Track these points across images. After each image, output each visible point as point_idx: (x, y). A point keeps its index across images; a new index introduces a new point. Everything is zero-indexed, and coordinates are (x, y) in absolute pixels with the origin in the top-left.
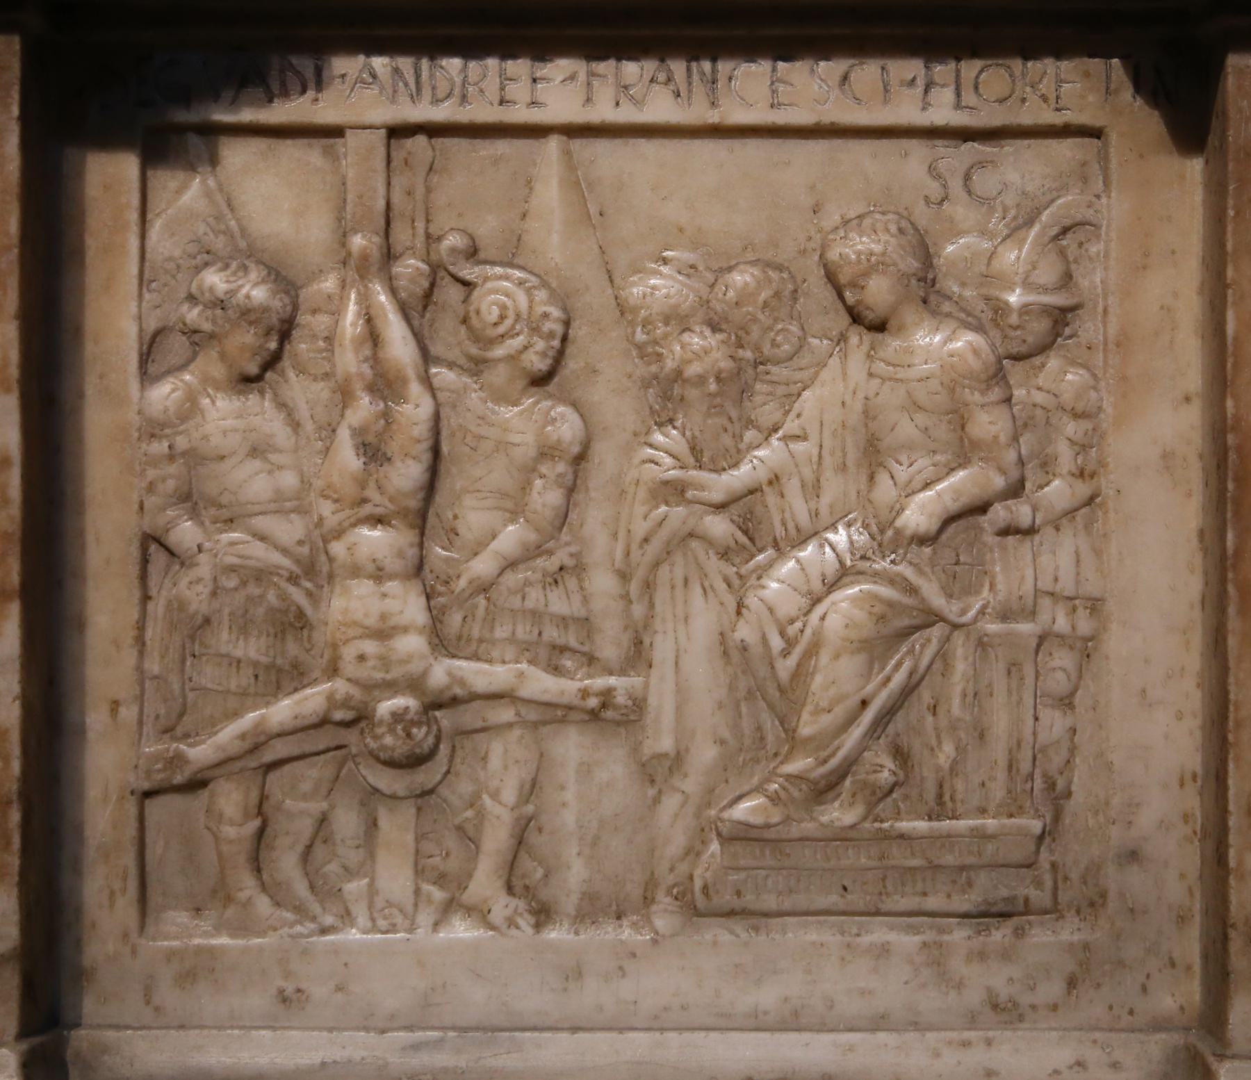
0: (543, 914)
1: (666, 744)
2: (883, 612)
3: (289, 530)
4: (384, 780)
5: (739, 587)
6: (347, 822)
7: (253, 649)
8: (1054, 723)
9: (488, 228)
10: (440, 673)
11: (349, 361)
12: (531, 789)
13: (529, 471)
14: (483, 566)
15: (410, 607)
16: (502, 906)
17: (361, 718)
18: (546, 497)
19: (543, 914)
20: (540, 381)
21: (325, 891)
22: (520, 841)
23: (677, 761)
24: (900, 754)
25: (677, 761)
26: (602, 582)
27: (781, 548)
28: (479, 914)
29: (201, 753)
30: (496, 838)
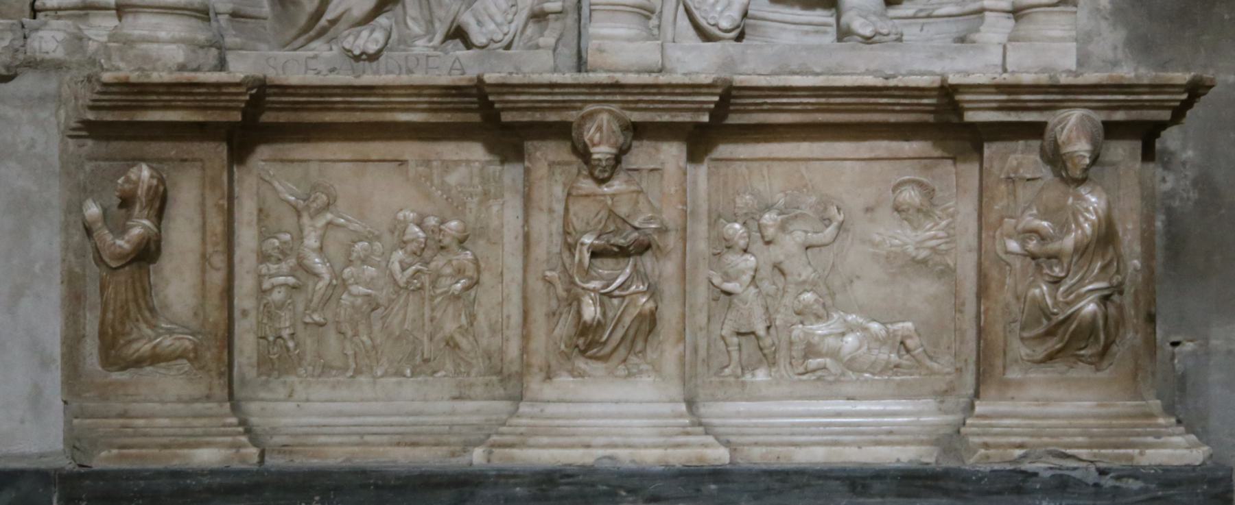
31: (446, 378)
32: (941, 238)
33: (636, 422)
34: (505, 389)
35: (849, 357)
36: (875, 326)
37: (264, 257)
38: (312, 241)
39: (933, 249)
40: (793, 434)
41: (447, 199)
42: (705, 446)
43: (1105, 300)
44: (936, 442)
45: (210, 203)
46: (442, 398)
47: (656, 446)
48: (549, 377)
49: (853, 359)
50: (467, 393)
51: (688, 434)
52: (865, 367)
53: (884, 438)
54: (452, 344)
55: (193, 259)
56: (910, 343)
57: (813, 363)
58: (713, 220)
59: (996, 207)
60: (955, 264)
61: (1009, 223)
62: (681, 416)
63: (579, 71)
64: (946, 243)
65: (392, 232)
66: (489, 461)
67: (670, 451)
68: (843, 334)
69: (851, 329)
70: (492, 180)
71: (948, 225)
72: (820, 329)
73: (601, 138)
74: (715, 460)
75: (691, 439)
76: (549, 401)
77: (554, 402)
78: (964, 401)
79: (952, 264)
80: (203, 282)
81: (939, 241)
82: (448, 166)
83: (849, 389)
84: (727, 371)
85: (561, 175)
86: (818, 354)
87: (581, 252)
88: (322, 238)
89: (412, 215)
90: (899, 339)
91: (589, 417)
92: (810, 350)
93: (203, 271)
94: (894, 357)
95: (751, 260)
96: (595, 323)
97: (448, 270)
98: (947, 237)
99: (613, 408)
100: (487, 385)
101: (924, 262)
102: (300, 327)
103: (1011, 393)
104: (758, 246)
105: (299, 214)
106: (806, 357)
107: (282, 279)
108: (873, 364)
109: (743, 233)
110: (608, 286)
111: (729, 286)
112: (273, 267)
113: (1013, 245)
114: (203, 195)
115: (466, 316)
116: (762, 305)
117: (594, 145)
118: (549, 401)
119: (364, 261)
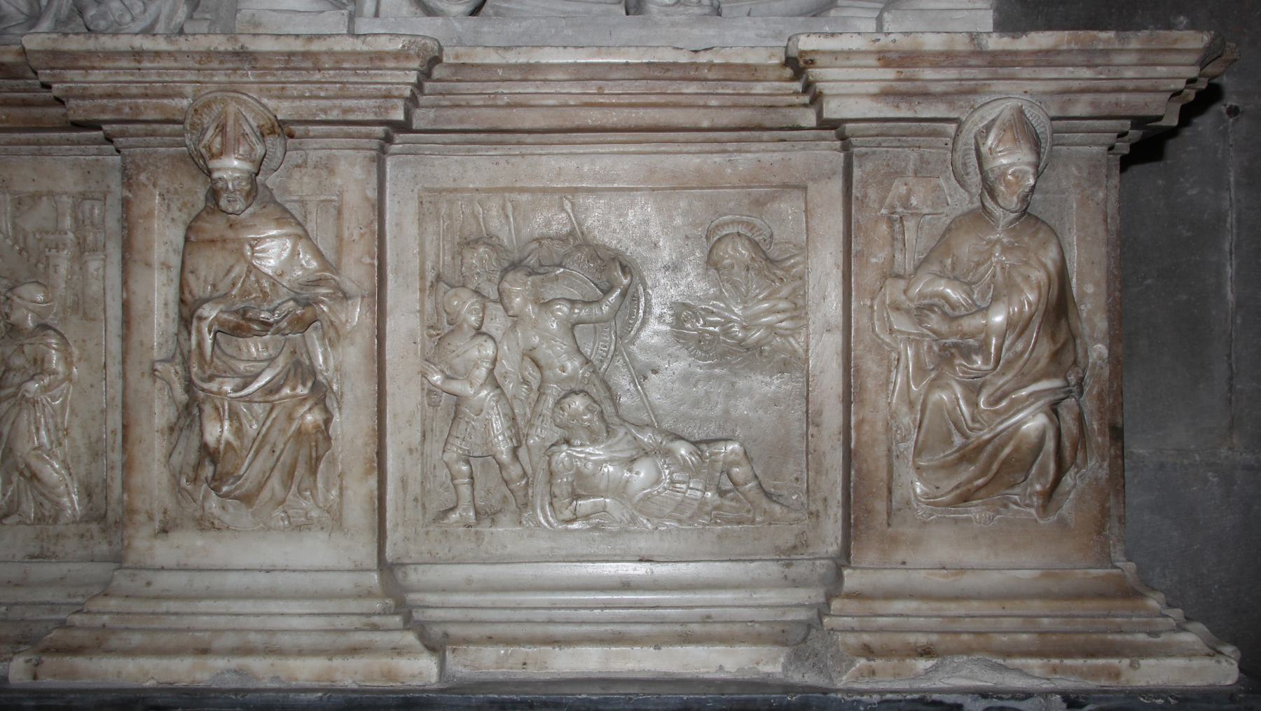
31: (21, 526)
32: (784, 311)
33: (294, 607)
34: (110, 543)
35: (641, 494)
39: (770, 327)
40: (551, 622)
41: (20, 252)
42: (398, 651)
43: (1053, 410)
46: (14, 556)
47: (316, 652)
49: (647, 498)
50: (52, 548)
51: (375, 628)
52: (668, 511)
53: (696, 628)
54: (27, 474)
57: (585, 505)
58: (428, 284)
59: (874, 260)
60: (807, 351)
62: (369, 594)
64: (792, 318)
66: (35, 677)
67: (338, 662)
68: (633, 460)
70: (88, 222)
71: (794, 290)
73: (223, 144)
74: (414, 676)
75: (378, 638)
76: (163, 568)
77: (171, 570)
78: (822, 567)
79: (801, 351)
81: (780, 316)
83: (642, 544)
84: (454, 516)
85: (180, 210)
87: (199, 331)
90: (719, 465)
92: (582, 487)
96: (222, 447)
98: (795, 309)
100: (82, 536)
103: (900, 555)
104: (497, 323)
106: (576, 496)
108: (680, 506)
109: (473, 304)
110: (245, 386)
115: (48, 431)
116: (505, 415)
117: (213, 156)
118: (163, 568)
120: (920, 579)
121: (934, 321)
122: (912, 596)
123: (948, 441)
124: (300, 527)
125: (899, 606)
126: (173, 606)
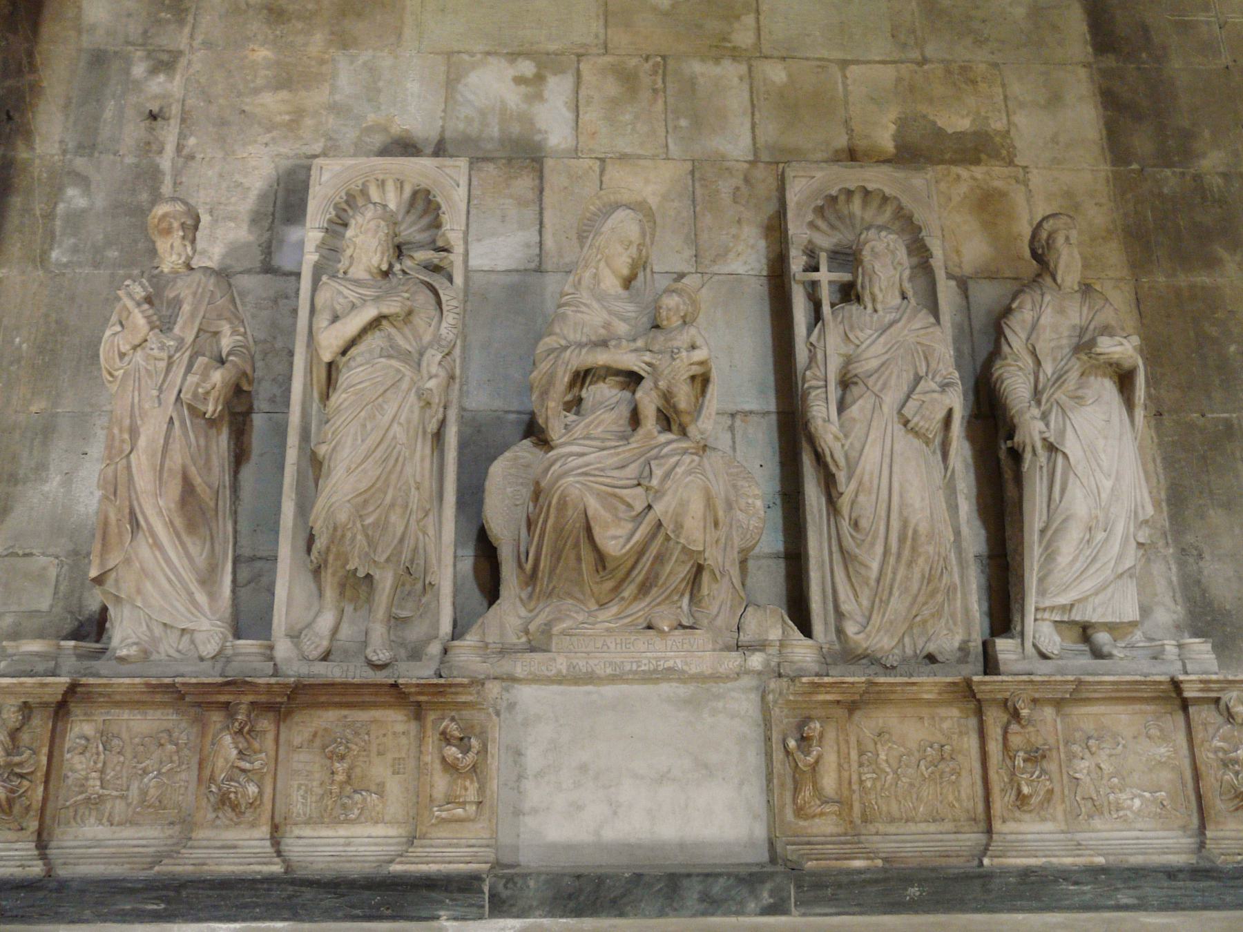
0: (112, 825)
1: (130, 801)
2: (158, 782)
3: (83, 773)
4: (92, 807)
5: (142, 779)
6: (87, 813)
7: (77, 789)
8: (181, 798)
9: (115, 732)
10: (101, 792)
11: (94, 750)
12: (112, 808)
13: (115, 766)
14: (108, 777)
15: (98, 783)
16: (106, 823)
17: (89, 798)
18: (118, 768)
19: (112, 825)
20: (119, 753)
21: (83, 821)
22: (110, 814)
23: (131, 803)
24: (160, 802)
25: (131, 803)
26: (125, 779)
27: (148, 774)
28: (103, 824)
29: (68, 804)
30: (107, 814)
36: (1147, 794)
37: (861, 765)
38: (883, 756)
44: (1193, 852)
45: (841, 738)
48: (1004, 822)
55: (834, 766)
56: (1165, 803)
57: (1121, 813)
61: (1207, 745)
63: (986, 673)
65: (919, 751)
69: (1134, 796)
72: (1123, 796)
80: (840, 777)
82: (943, 719)
83: (1138, 826)
84: (1081, 817)
86: (1123, 809)
88: (887, 755)
89: (927, 743)
91: (1028, 841)
93: (840, 771)
94: (1158, 810)
95: (1087, 764)
97: (947, 769)
99: (1038, 836)
101: (1165, 763)
102: (879, 798)
104: (1087, 755)
105: (876, 744)
106: (1117, 810)
107: (869, 776)
111: (1077, 775)
112: (866, 770)
113: (1211, 755)
114: (837, 735)
119: (907, 766)
120: (1228, 834)
121: (1221, 755)
122: (1232, 839)
123: (1230, 791)
124: (1043, 820)
125: (1226, 842)
126: (1026, 844)
